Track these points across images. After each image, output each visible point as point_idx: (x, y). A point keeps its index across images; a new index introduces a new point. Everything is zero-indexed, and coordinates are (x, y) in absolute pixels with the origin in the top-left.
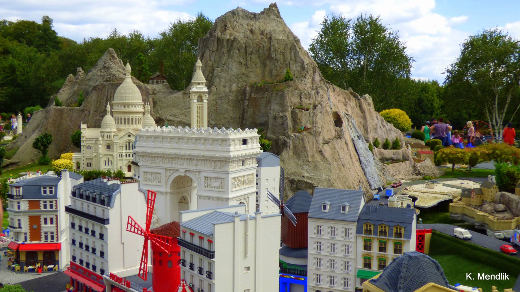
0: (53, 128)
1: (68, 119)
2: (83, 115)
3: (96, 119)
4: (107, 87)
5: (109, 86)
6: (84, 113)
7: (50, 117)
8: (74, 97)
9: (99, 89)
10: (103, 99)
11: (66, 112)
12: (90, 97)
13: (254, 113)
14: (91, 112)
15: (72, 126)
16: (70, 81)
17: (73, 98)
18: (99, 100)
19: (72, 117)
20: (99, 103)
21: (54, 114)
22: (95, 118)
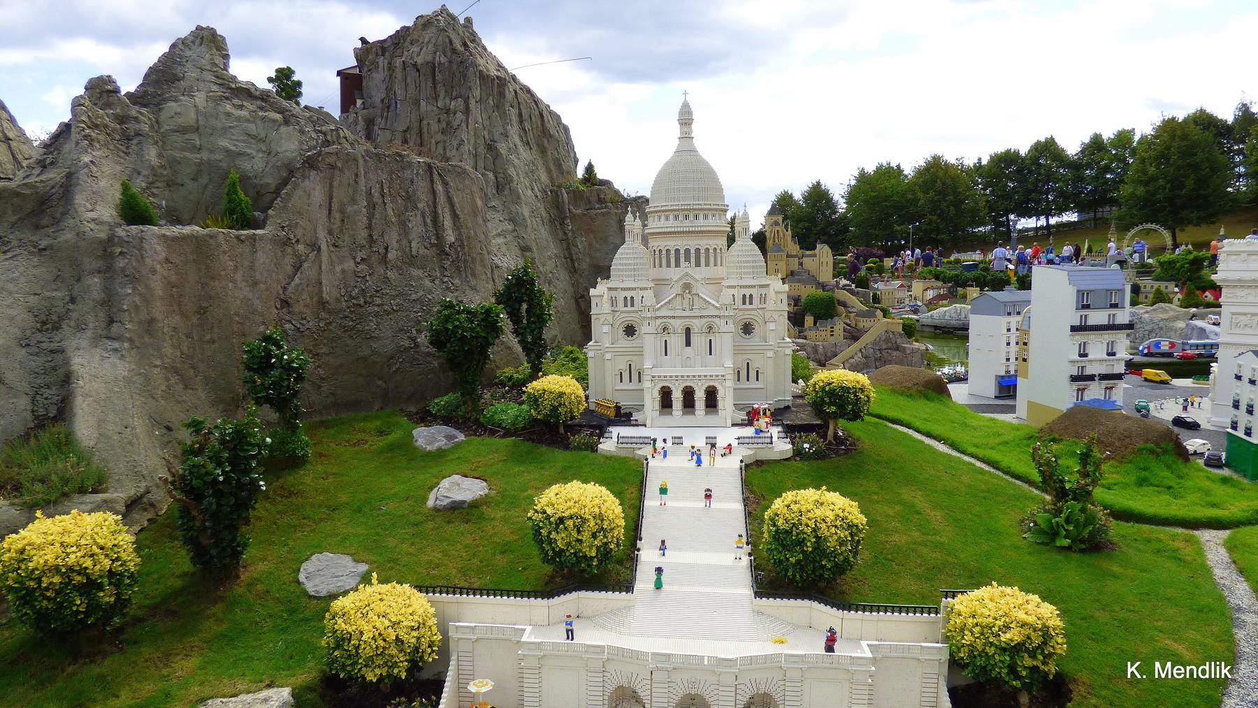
0: (176, 320)
1: (239, 276)
2: (289, 261)
3: (343, 271)
4: (361, 162)
5: (365, 161)
6: (289, 250)
7: (154, 271)
8: (155, 191)
9: (332, 167)
10: (353, 201)
11: (225, 247)
12: (299, 193)
13: (591, 245)
14: (324, 247)
15: (257, 302)
16: (97, 126)
17: (154, 195)
18: (335, 206)
19: (252, 268)
20: (338, 216)
21: (167, 260)
22: (338, 269)
